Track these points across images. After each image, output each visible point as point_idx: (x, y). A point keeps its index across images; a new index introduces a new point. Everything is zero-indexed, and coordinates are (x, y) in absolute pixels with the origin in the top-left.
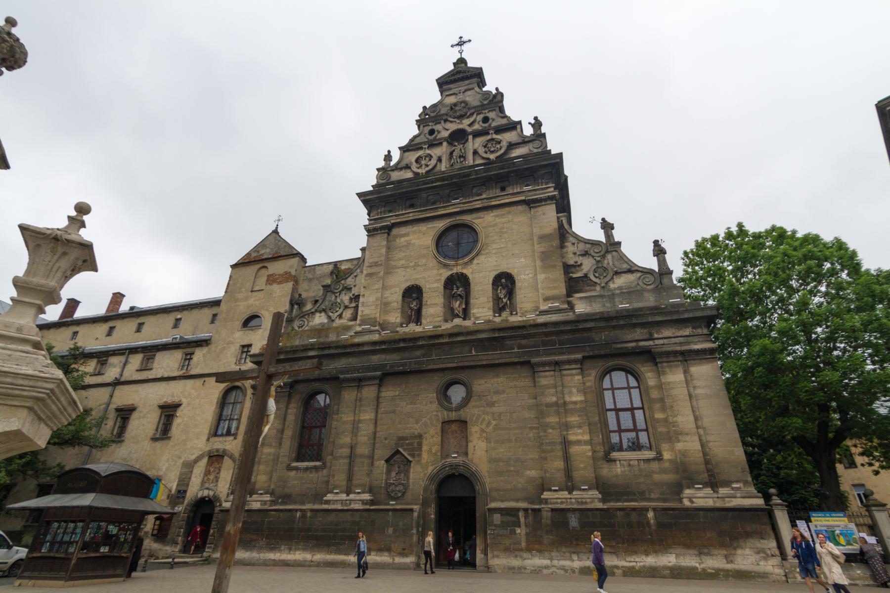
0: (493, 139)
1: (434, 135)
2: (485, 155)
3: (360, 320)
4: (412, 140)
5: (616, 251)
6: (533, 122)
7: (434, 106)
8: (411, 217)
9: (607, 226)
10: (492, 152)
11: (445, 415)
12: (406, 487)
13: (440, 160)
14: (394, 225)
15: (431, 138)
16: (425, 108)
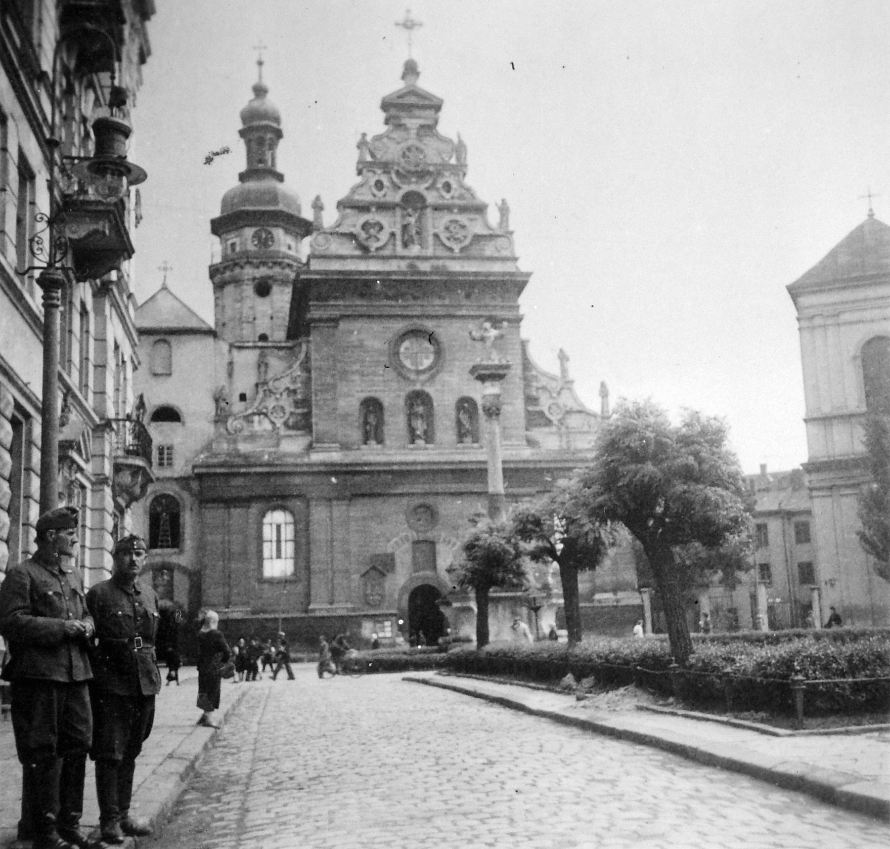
0: (457, 222)
1: (383, 192)
2: (448, 244)
3: (317, 434)
4: (354, 191)
5: (569, 389)
6: (500, 203)
7: (378, 138)
8: (363, 310)
9: (563, 357)
10: (455, 239)
11: (413, 535)
12: (382, 596)
13: (393, 235)
14: (343, 317)
15: (380, 194)
16: (364, 135)
